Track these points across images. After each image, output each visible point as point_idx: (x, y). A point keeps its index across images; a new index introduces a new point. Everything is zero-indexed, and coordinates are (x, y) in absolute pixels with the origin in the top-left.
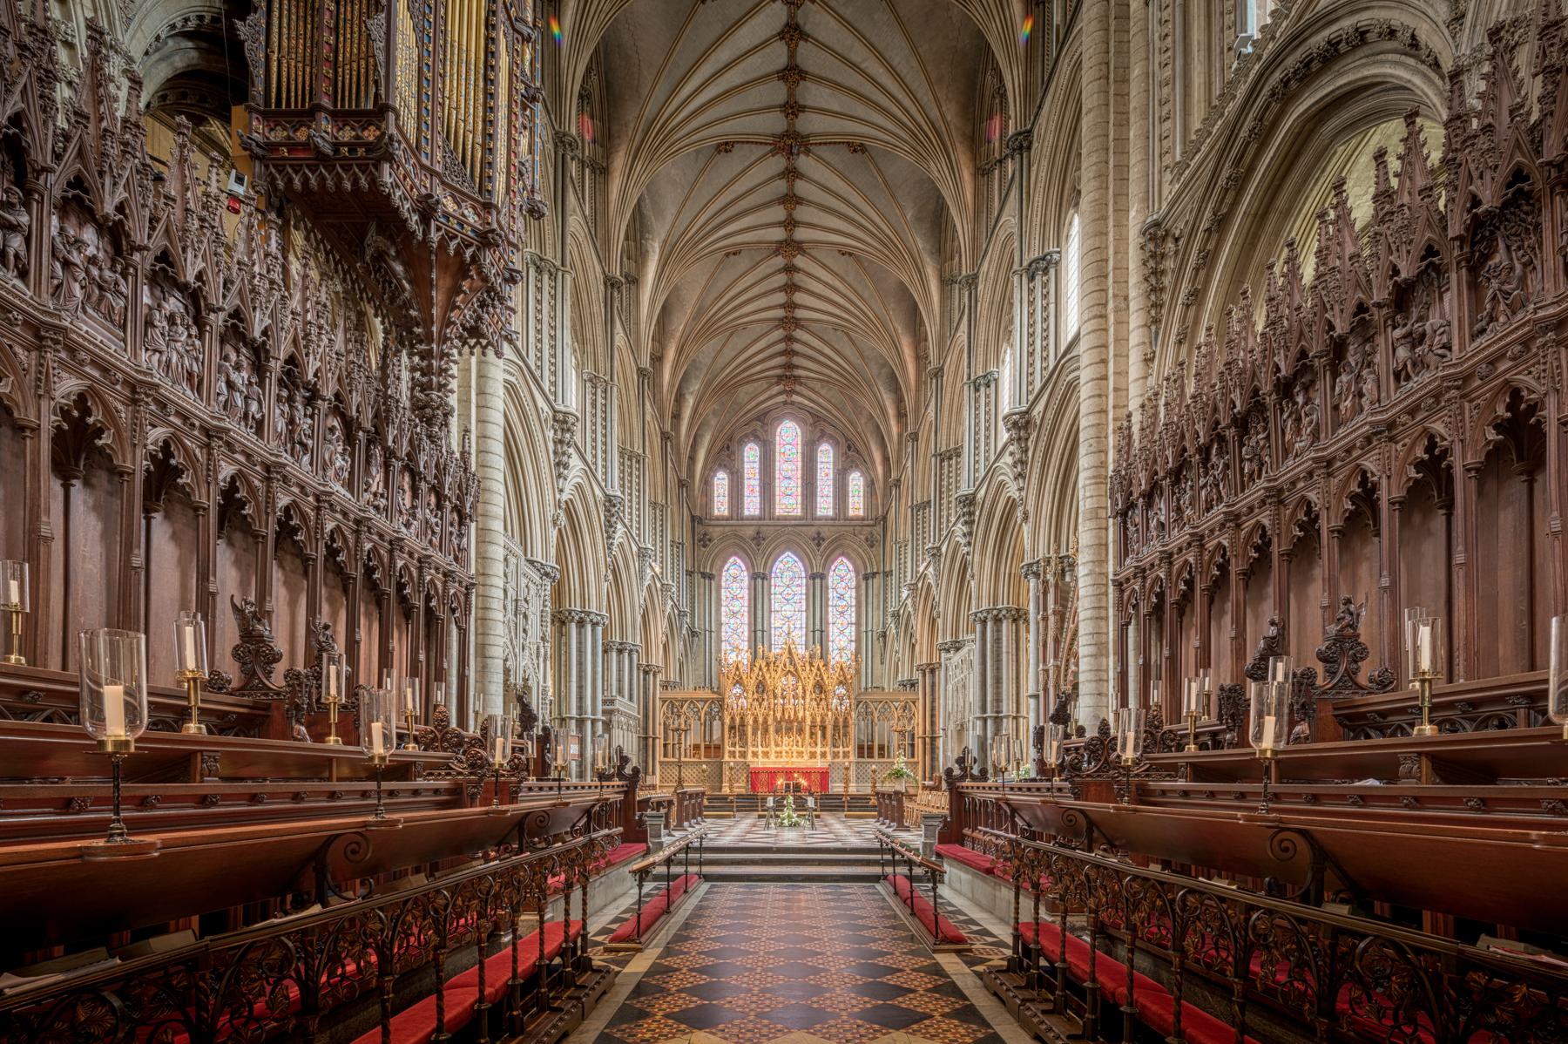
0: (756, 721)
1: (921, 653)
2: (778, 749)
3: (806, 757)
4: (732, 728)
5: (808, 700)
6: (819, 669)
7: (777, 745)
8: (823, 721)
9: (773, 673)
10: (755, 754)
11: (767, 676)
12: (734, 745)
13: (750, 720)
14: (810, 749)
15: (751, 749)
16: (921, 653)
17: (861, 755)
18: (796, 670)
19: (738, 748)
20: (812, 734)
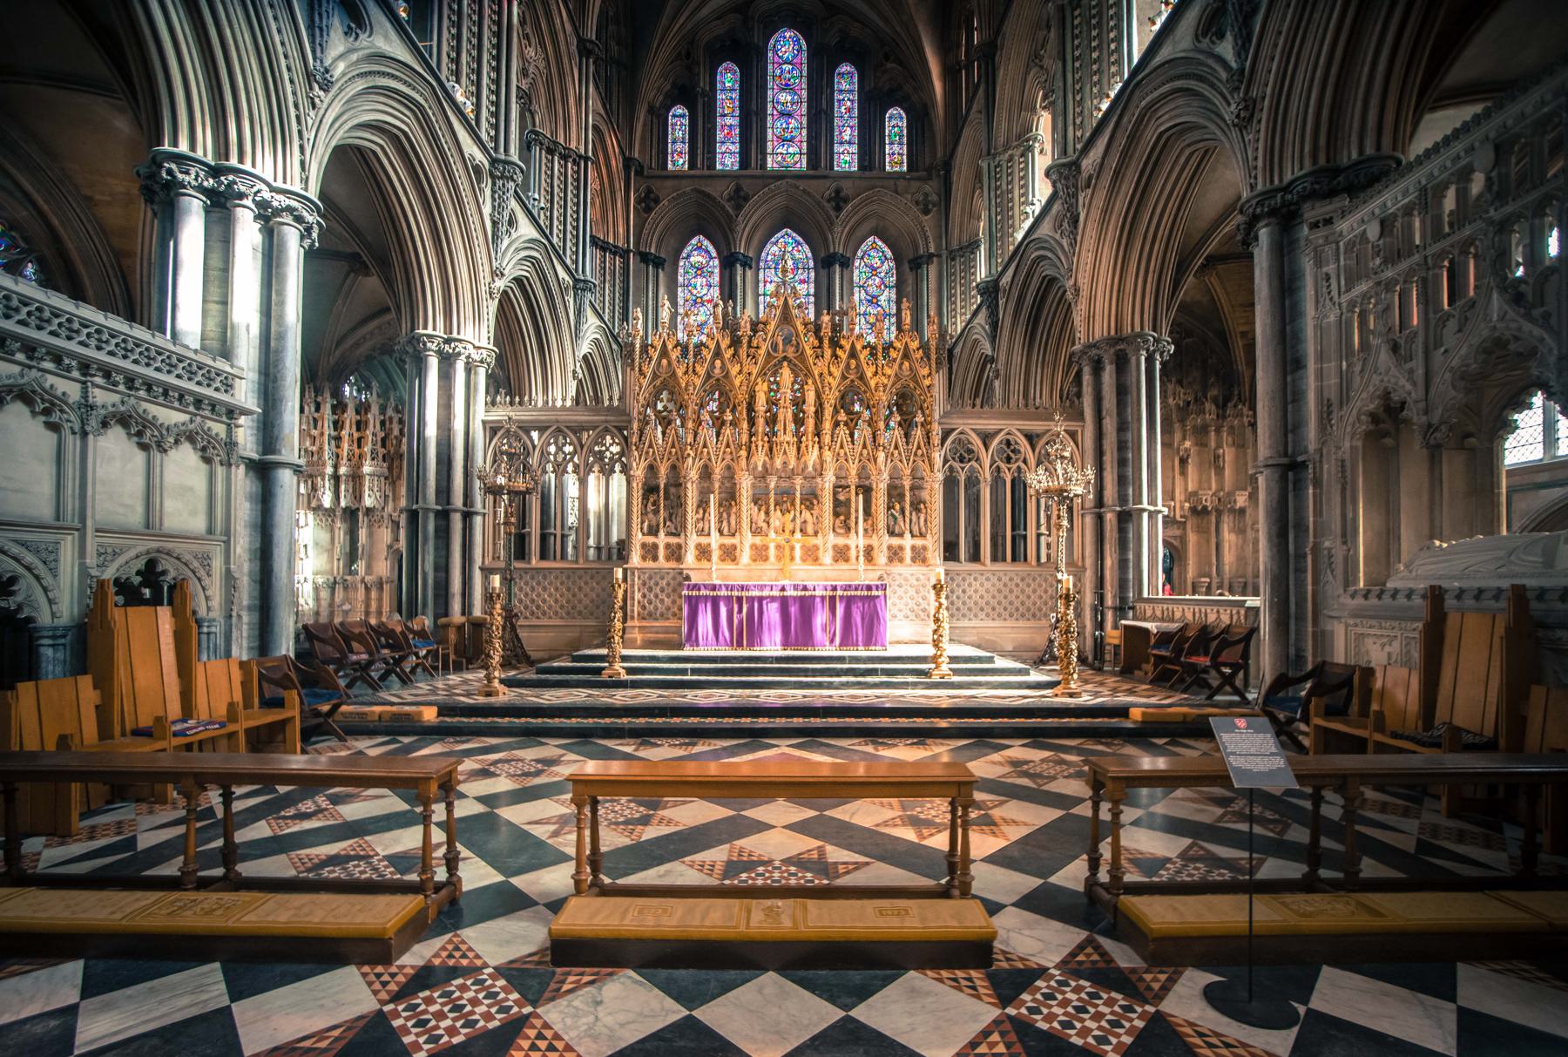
0: (706, 473)
1: (1090, 318)
2: (758, 540)
3: (827, 558)
4: (650, 490)
5: (827, 426)
6: (853, 354)
7: (756, 531)
8: (863, 474)
9: (749, 366)
10: (704, 553)
11: (734, 370)
12: (653, 531)
13: (692, 473)
14: (832, 539)
15: (693, 540)
16: (1090, 318)
17: (950, 552)
18: (802, 356)
19: (662, 539)
20: (841, 508)
